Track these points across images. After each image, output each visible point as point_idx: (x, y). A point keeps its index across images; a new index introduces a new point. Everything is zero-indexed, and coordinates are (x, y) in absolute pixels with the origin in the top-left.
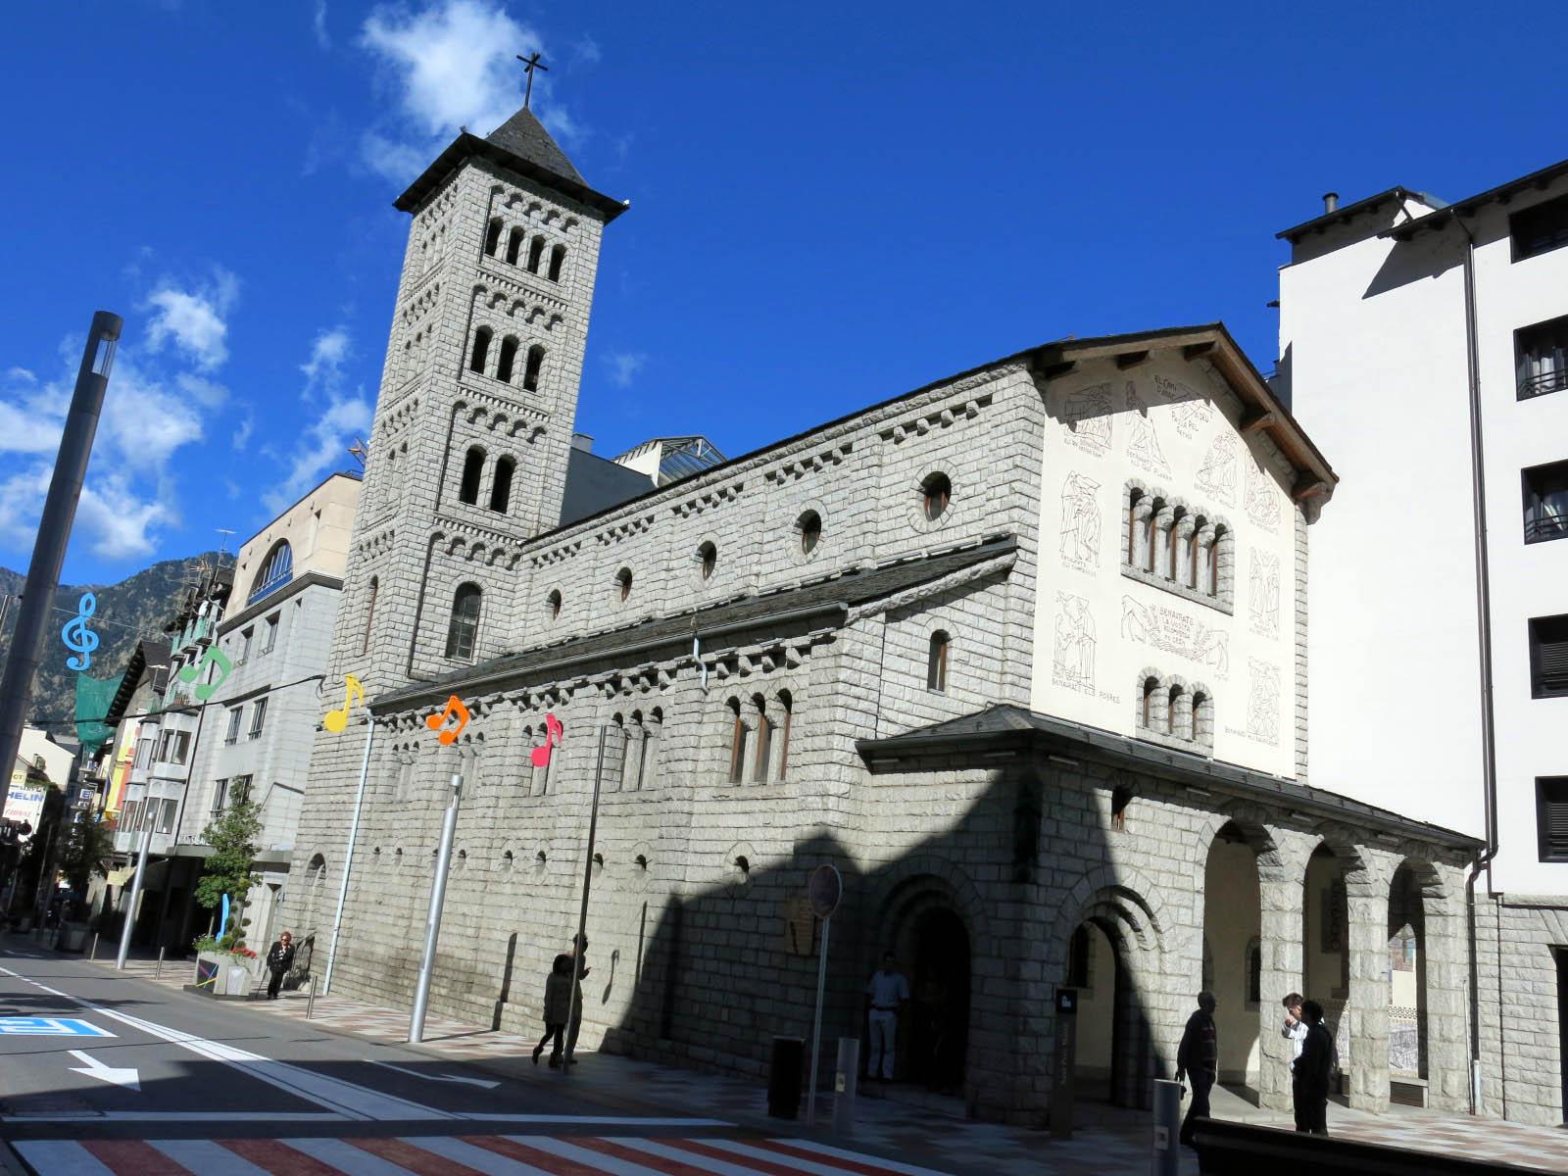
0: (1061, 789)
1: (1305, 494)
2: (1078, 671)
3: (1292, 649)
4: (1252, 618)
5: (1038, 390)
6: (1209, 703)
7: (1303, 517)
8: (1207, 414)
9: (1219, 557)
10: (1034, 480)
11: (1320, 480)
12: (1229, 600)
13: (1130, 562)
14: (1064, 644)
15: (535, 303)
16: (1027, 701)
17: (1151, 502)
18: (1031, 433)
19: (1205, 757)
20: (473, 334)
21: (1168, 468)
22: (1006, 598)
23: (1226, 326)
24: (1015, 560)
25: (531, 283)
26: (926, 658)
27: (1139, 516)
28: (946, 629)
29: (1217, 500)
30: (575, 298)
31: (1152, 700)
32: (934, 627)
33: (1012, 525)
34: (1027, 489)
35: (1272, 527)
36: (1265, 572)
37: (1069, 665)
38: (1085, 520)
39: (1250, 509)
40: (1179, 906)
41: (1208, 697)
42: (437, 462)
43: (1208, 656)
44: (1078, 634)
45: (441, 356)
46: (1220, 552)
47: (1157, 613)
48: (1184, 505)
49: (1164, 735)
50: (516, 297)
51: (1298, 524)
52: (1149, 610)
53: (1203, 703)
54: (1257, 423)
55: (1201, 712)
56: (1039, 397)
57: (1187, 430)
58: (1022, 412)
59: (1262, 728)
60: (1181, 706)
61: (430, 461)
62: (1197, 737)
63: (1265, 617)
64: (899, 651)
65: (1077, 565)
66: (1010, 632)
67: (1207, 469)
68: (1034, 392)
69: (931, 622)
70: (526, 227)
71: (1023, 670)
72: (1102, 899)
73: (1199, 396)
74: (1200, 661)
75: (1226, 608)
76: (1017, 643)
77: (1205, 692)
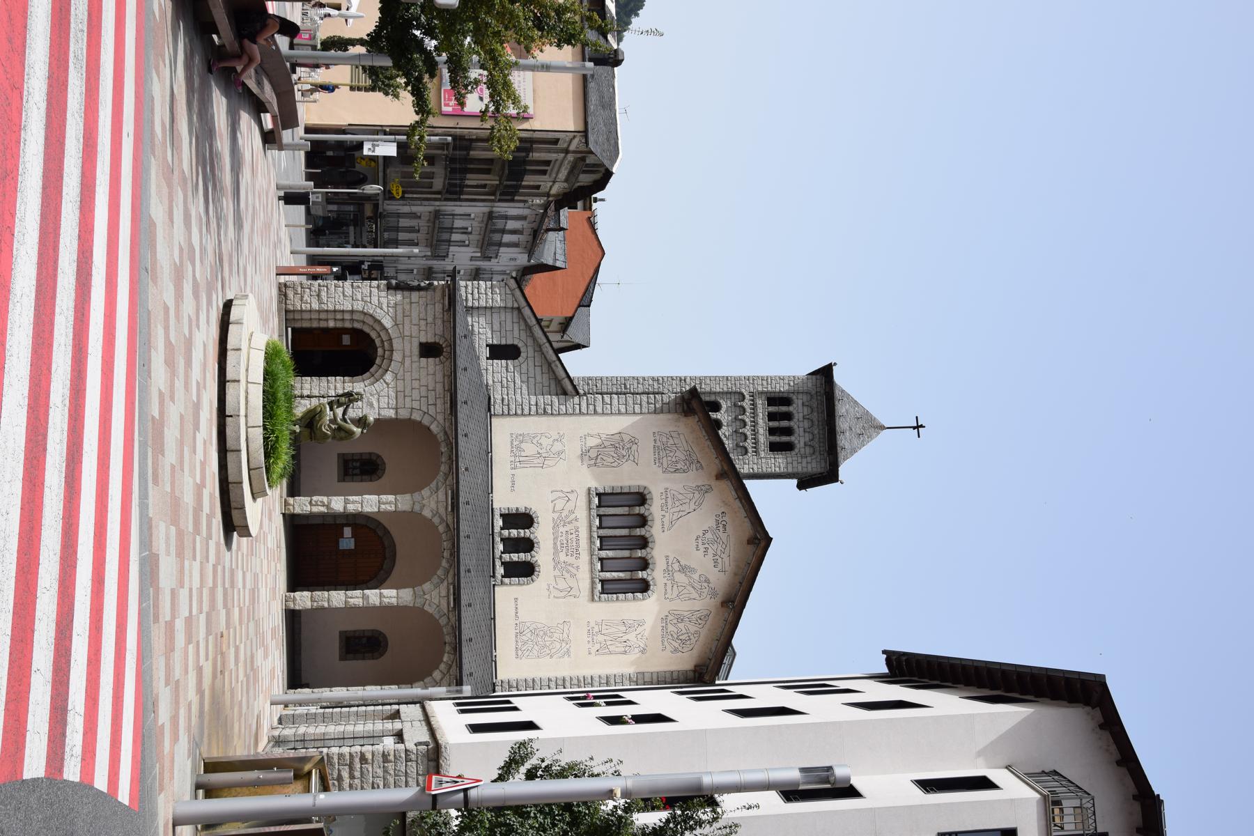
0: (435, 304)
10: (623, 409)
14: (535, 441)
15: (748, 433)
20: (712, 398)
25: (761, 431)
26: (503, 342)
28: (522, 354)
29: (666, 582)
30: (764, 460)
32: (520, 345)
36: (631, 636)
37: (523, 446)
38: (612, 454)
40: (388, 397)
42: (626, 388)
43: (559, 577)
45: (691, 379)
50: (747, 420)
52: (573, 516)
57: (702, 548)
59: (524, 638)
61: (625, 384)
63: (600, 638)
64: (503, 323)
65: (584, 448)
67: (683, 569)
69: (523, 344)
70: (795, 420)
72: (386, 343)
77: (536, 573)
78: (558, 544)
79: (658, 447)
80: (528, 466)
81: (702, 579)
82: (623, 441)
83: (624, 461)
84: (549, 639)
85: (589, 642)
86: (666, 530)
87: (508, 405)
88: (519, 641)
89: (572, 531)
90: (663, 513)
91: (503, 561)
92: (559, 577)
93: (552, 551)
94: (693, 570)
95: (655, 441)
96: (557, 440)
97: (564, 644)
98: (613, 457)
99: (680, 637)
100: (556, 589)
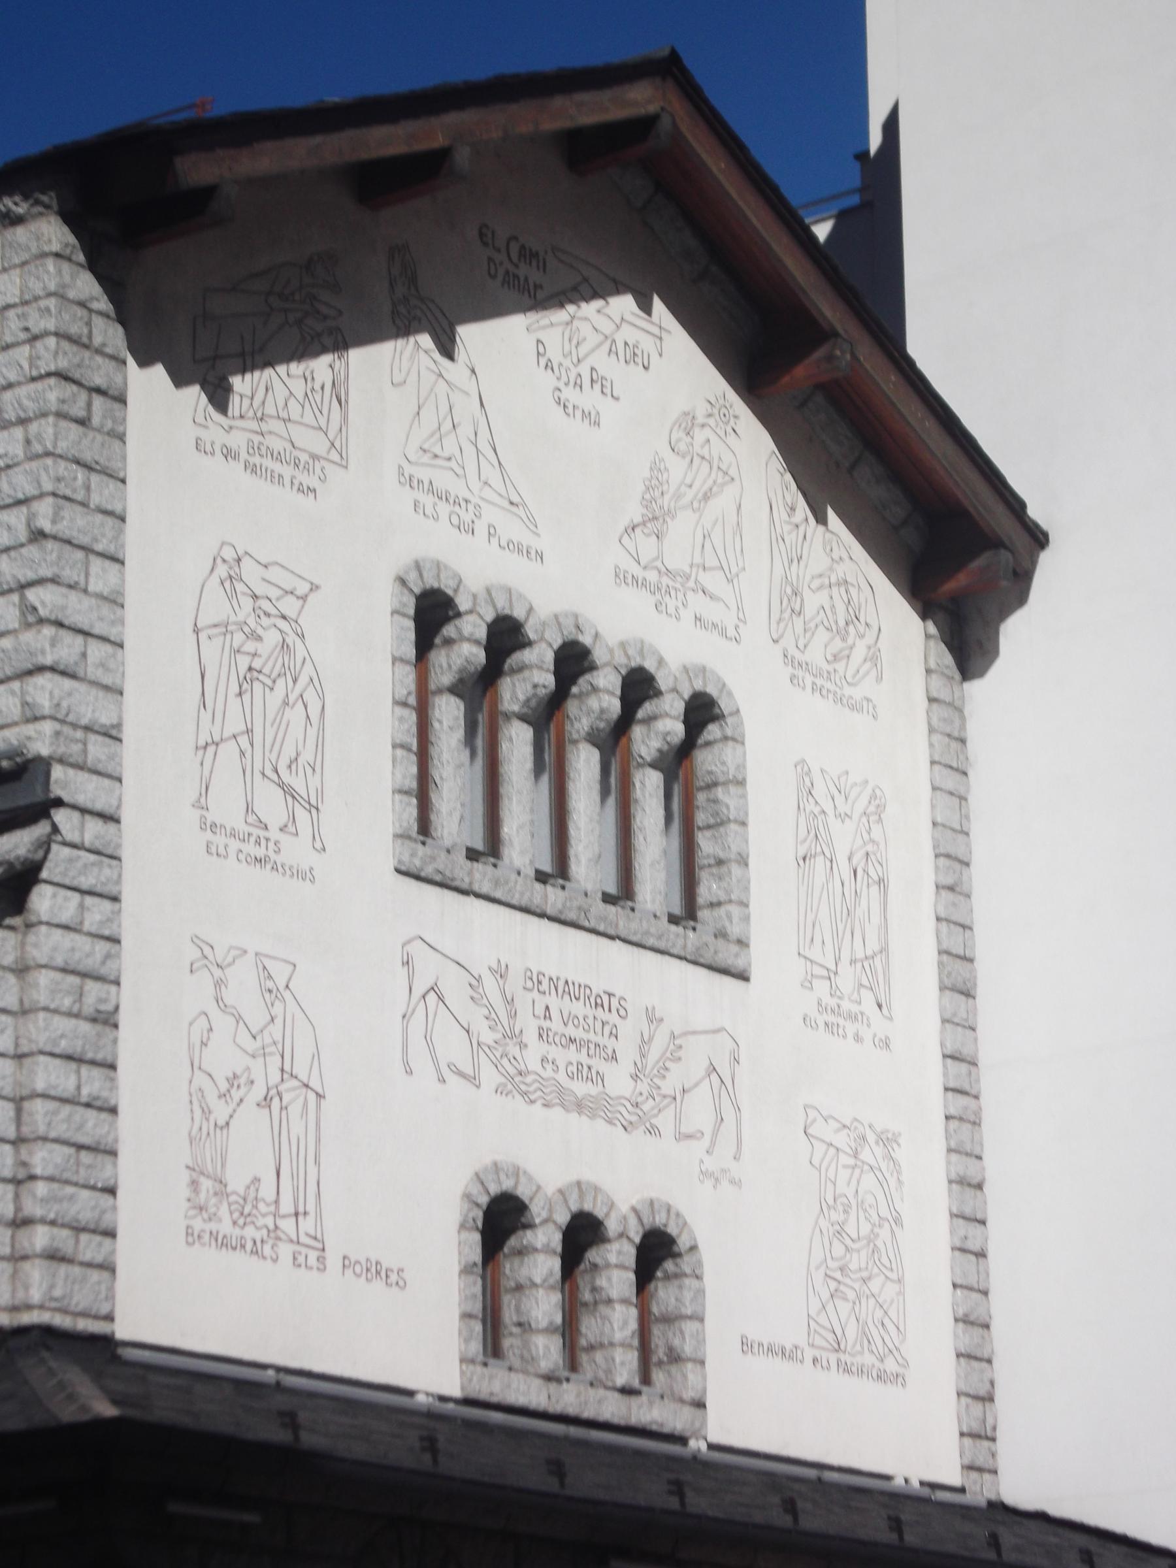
1: (951, 586)
2: (267, 1191)
3: (933, 1074)
4: (808, 984)
5: (101, 278)
6: (686, 1265)
7: (949, 660)
8: (647, 344)
9: (701, 798)
10: (101, 577)
11: (995, 543)
12: (735, 930)
13: (424, 827)
14: (221, 1112)
16: (104, 1309)
17: (482, 633)
18: (83, 422)
19: (682, 1440)
21: (532, 525)
22: (22, 970)
23: (688, 61)
24: (45, 845)
27: (447, 679)
29: (687, 616)
31: (512, 1270)
33: (30, 729)
34: (78, 609)
35: (857, 693)
37: (237, 1183)
39: (788, 642)
41: (683, 1243)
43: (678, 1119)
44: (265, 1073)
46: (701, 779)
47: (515, 983)
48: (586, 639)
49: (549, 1378)
51: (939, 687)
53: (669, 1265)
54: (800, 371)
55: (664, 1295)
56: (103, 304)
57: (589, 399)
58: (50, 354)
59: (852, 1331)
60: (602, 1282)
62: (658, 1376)
63: (847, 979)
65: (250, 848)
66: (40, 1086)
68: (86, 285)
71: (84, 1205)
73: (618, 288)
74: (653, 1131)
75: (727, 954)
76: (64, 1121)
77: (672, 1230)
78: (581, 1088)
79: (253, 449)
80: (312, 1170)
81: (682, 447)
82: (224, 627)
83: (301, 652)
84: (853, 1212)
85: (858, 1038)
86: (535, 544)
87: (78, 1229)
88: (858, 1360)
89: (540, 1011)
90: (481, 528)
91: (636, 1383)
92: (678, 1119)
93: (600, 1124)
94: (657, 467)
95: (229, 454)
96: (219, 984)
97: (866, 1155)
98: (286, 703)
99: (842, 623)
100: (713, 1143)
